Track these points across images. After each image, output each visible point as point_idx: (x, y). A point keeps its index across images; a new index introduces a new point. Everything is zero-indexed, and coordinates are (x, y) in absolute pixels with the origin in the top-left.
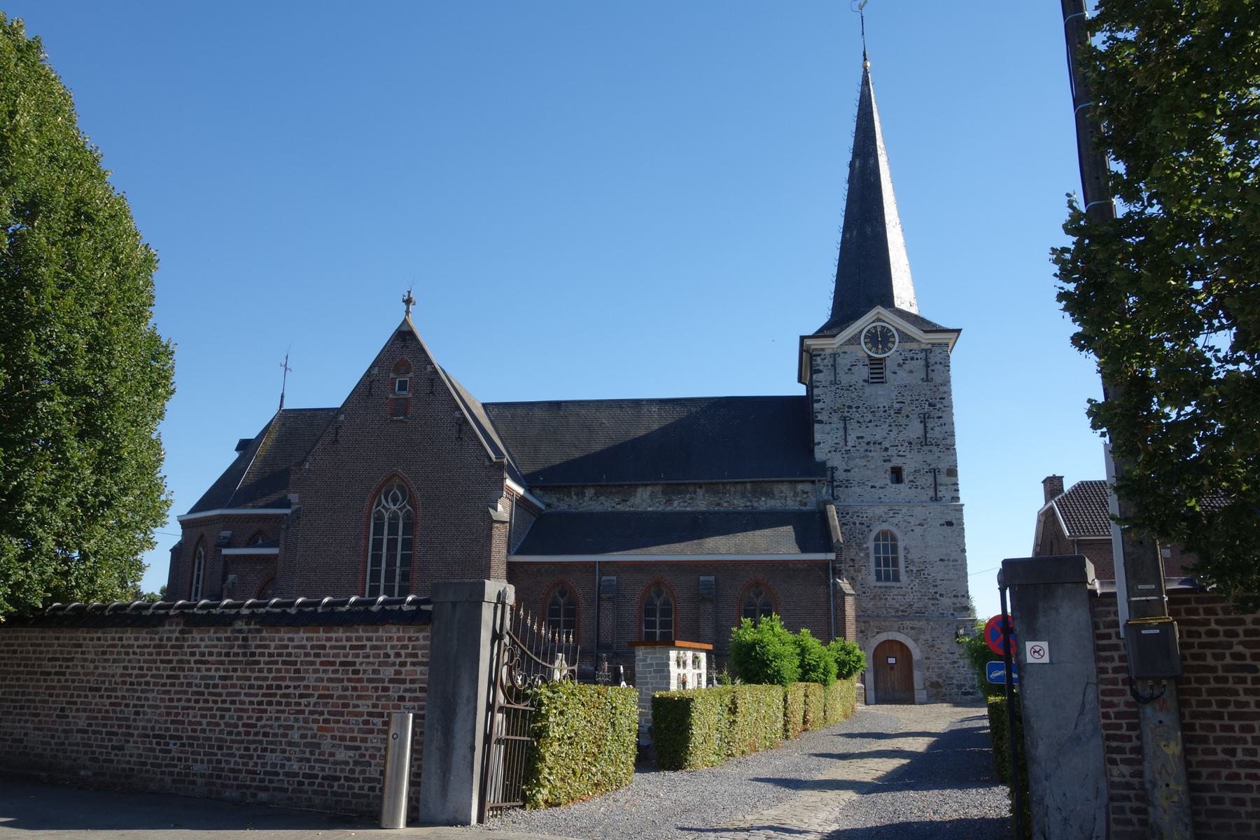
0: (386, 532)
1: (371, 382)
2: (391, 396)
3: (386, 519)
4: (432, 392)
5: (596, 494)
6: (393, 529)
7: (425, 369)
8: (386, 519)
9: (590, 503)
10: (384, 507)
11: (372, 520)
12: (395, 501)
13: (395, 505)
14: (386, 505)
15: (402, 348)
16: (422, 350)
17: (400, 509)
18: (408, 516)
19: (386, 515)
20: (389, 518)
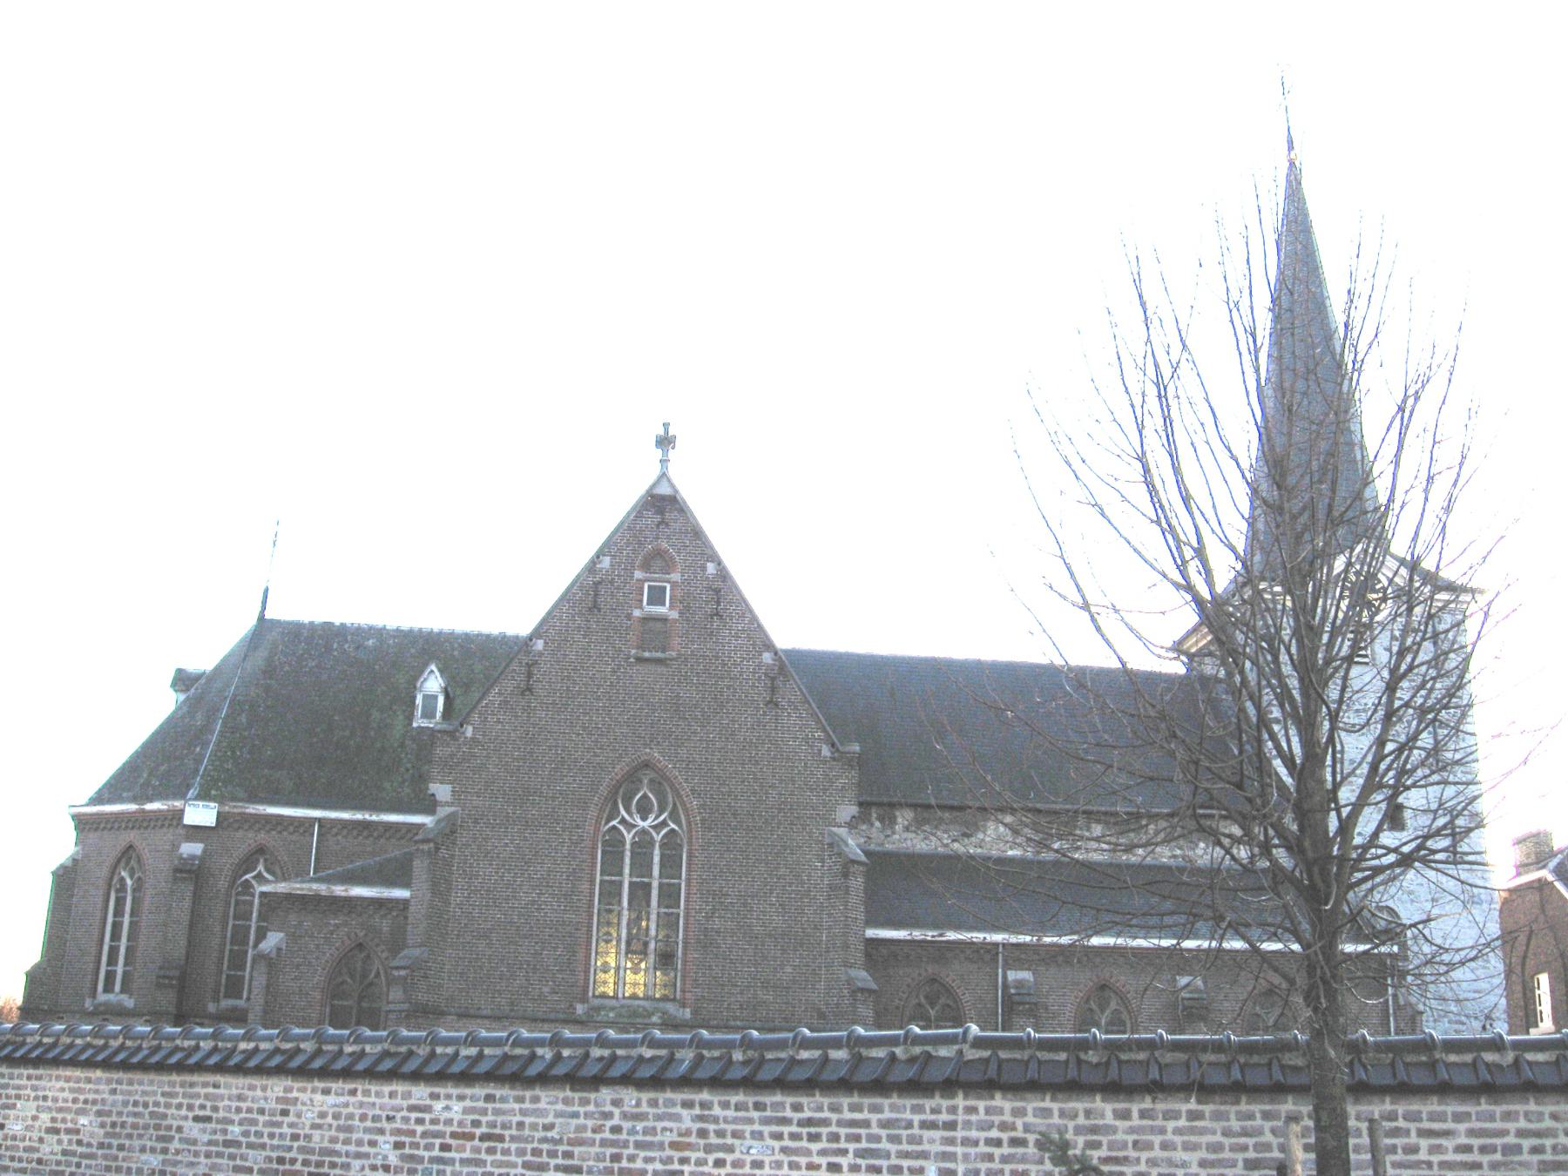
0: (627, 870)
1: (597, 584)
2: (637, 613)
3: (628, 846)
4: (717, 614)
5: (916, 819)
6: (642, 863)
7: (704, 568)
8: (628, 846)
9: (906, 835)
10: (623, 821)
11: (600, 845)
12: (644, 812)
13: (644, 819)
14: (627, 817)
15: (658, 526)
16: (697, 534)
17: (657, 828)
18: (671, 841)
19: (628, 837)
20: (633, 844)
